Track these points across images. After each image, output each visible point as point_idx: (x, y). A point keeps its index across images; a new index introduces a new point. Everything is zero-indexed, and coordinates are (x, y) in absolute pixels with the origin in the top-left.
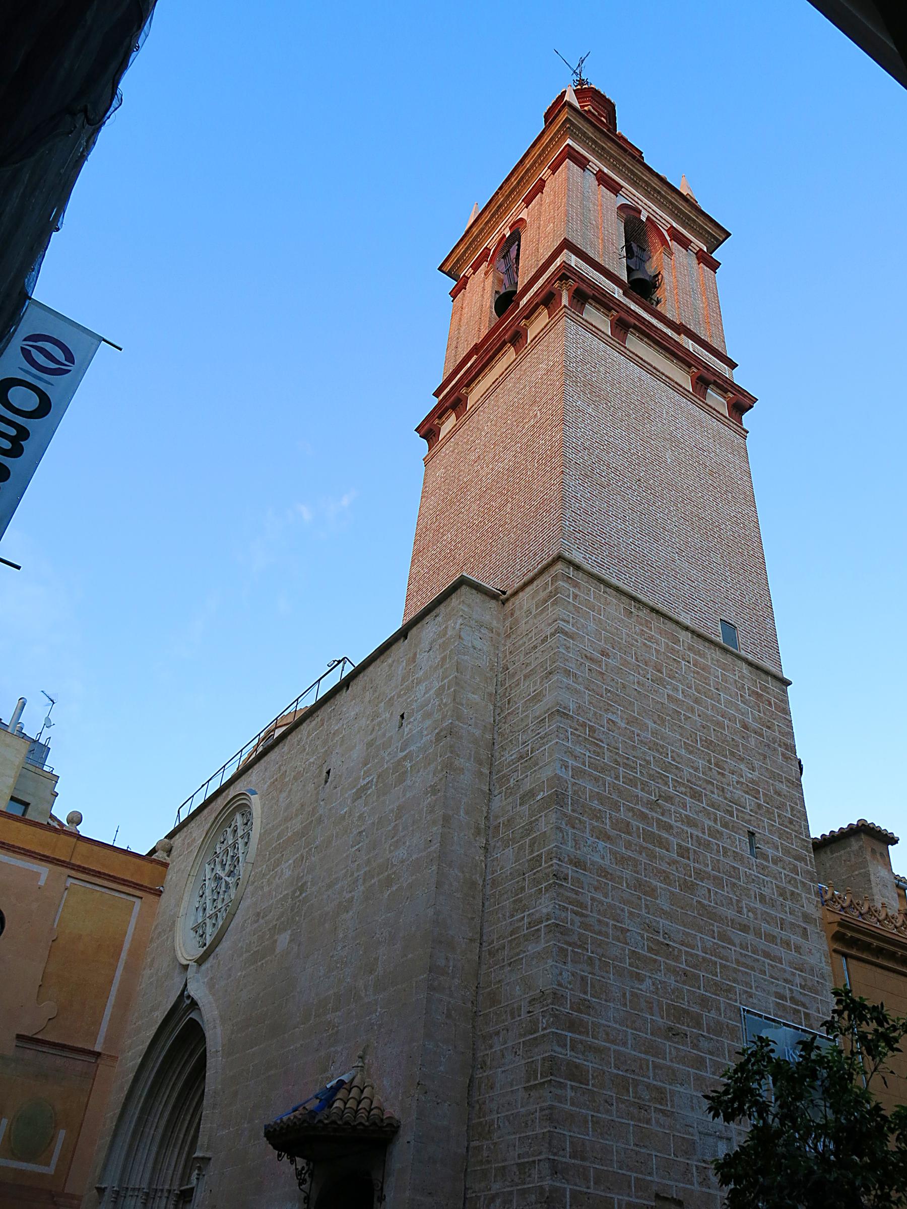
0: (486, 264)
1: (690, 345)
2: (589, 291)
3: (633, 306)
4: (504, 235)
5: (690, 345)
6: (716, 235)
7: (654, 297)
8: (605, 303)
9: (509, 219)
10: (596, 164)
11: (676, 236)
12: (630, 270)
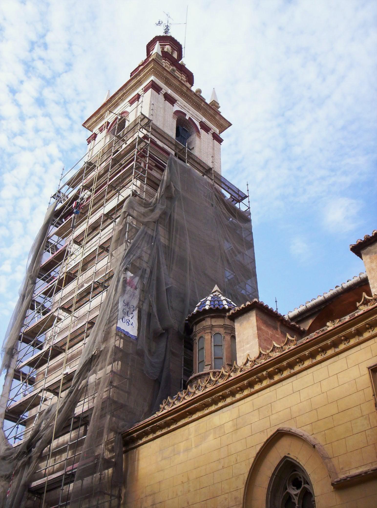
11: (203, 125)
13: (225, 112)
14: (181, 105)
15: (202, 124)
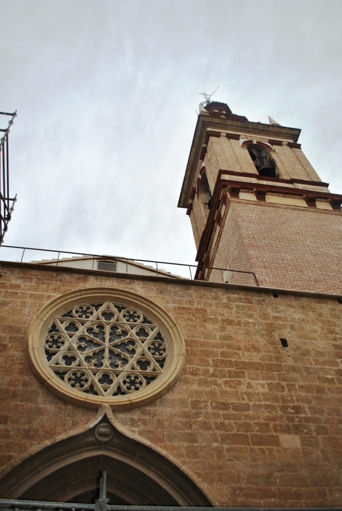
0: (196, 195)
1: (300, 186)
2: (239, 186)
3: (265, 183)
4: (199, 178)
5: (300, 186)
6: (294, 134)
7: (275, 174)
8: (248, 187)
9: (198, 171)
10: (224, 132)
12: (257, 167)
13: (285, 122)
14: (244, 137)
15: (270, 141)
